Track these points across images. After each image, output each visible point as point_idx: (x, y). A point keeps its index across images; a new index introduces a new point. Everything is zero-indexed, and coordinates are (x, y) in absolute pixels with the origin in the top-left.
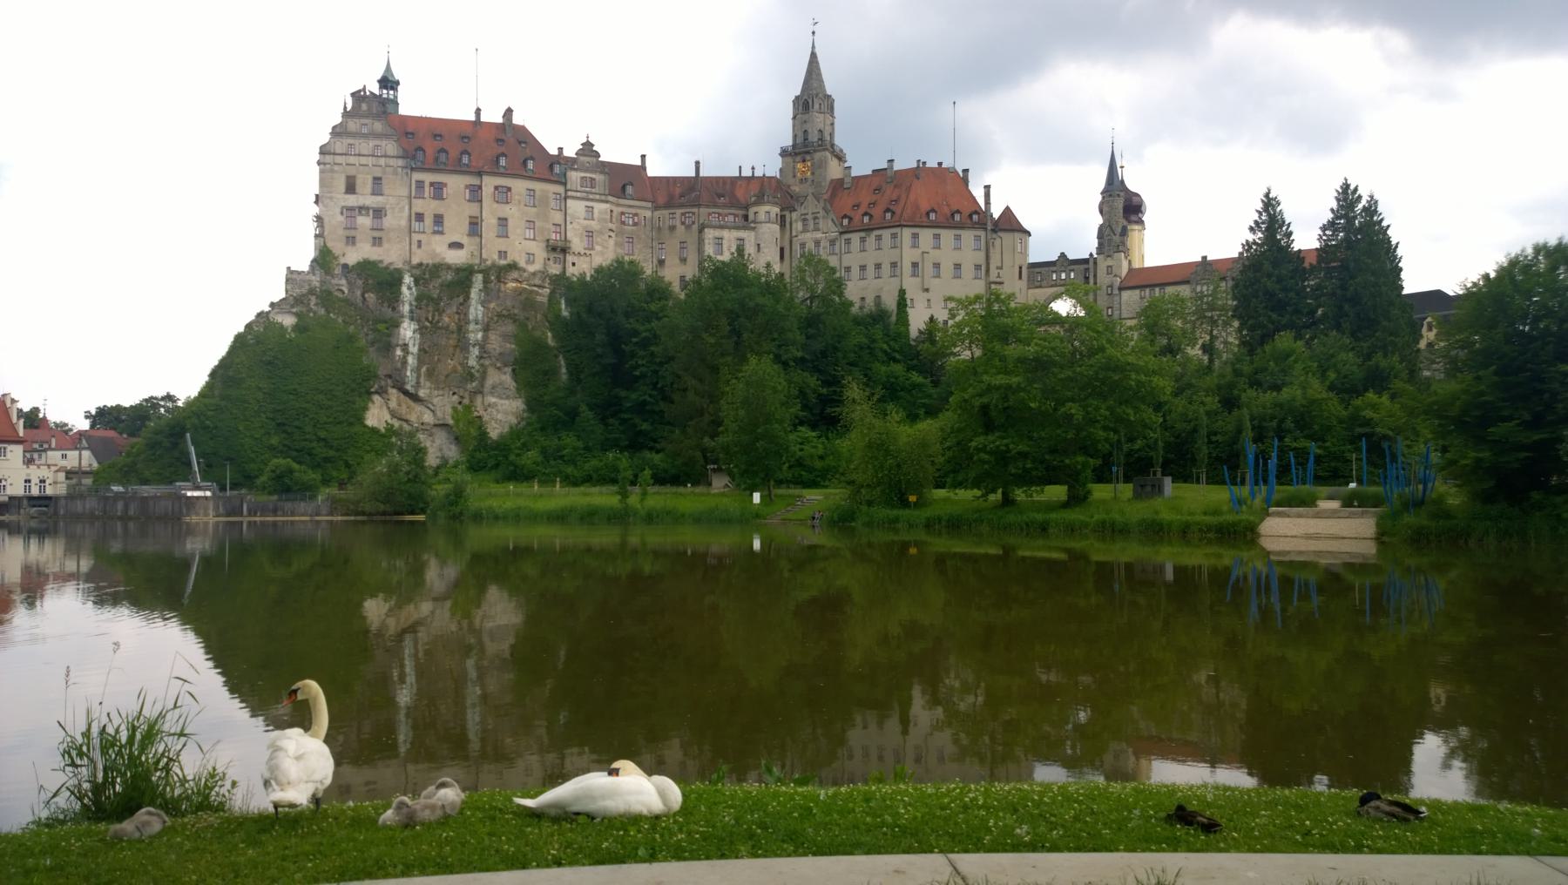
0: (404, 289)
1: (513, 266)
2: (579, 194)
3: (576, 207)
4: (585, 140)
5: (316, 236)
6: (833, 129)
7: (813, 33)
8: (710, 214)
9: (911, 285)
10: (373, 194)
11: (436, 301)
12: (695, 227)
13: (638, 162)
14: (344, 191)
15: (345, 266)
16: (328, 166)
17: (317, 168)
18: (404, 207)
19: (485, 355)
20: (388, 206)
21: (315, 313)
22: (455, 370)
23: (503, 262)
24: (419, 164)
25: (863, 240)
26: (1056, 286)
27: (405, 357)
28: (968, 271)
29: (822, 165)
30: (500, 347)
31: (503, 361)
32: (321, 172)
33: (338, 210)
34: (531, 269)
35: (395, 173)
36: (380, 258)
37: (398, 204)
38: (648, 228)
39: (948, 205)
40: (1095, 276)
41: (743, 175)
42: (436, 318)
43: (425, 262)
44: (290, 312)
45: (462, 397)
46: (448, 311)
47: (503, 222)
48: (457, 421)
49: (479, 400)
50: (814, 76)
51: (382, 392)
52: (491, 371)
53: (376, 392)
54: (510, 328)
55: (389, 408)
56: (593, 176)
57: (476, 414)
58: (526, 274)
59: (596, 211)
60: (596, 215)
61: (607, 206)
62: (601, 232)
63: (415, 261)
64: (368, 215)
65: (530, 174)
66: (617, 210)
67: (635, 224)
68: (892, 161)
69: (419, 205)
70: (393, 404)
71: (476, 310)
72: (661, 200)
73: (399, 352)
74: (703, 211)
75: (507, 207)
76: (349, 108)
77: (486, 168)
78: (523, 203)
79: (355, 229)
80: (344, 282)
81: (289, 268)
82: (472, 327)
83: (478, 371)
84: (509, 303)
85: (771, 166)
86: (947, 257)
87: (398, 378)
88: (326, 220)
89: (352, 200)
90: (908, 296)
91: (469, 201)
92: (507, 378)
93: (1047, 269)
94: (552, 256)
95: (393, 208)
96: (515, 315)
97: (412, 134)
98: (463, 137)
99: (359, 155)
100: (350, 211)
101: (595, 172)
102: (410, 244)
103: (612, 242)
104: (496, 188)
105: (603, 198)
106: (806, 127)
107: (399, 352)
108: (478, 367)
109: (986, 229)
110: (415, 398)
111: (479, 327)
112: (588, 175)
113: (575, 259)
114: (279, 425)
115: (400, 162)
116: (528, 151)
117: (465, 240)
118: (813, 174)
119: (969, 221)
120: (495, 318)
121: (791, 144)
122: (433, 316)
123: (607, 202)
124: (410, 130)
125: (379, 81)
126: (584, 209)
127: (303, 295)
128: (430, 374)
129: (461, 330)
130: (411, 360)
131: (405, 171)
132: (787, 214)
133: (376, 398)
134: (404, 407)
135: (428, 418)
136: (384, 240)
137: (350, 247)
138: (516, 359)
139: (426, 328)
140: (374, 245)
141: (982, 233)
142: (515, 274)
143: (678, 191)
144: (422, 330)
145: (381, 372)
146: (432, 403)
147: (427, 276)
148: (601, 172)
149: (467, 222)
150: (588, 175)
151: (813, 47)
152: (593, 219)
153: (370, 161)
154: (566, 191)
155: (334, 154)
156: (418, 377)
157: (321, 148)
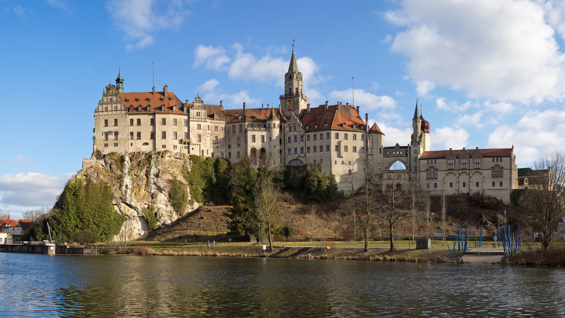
0: (126, 163)
15: (104, 155)
23: (163, 150)
26: (394, 157)
29: (297, 103)
34: (175, 151)
37: (123, 129)
40: (410, 154)
56: (200, 111)
59: (202, 126)
68: (327, 102)
69: (131, 129)
71: (153, 171)
85: (276, 104)
93: (391, 150)
95: (121, 131)
118: (294, 107)
121: (284, 94)
123: (206, 122)
126: (197, 125)
127: (88, 168)
137: (106, 148)
140: (115, 145)
142: (168, 154)
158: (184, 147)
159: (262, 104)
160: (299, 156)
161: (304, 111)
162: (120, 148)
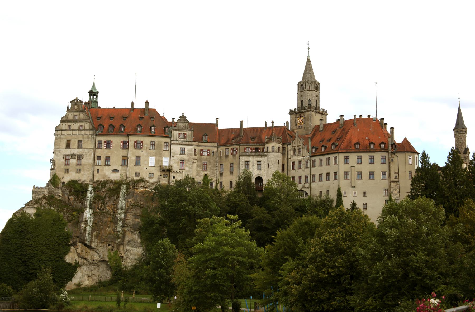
0: (88, 194)
1: (142, 180)
2: (177, 142)
3: (176, 149)
4: (181, 115)
5: (51, 169)
6: (318, 99)
7: (309, 49)
8: (245, 148)
9: (344, 185)
10: (78, 148)
11: (104, 199)
12: (237, 155)
13: (215, 122)
14: (65, 147)
15: (64, 183)
16: (59, 136)
17: (54, 136)
18: (91, 154)
19: (125, 225)
20: (84, 154)
21: (44, 207)
22: (110, 233)
23: (136, 178)
24: (100, 132)
25: (321, 160)
27: (85, 227)
28: (378, 175)
31: (135, 228)
32: (56, 139)
33: (62, 156)
34: (152, 181)
35: (88, 138)
37: (89, 152)
38: (215, 157)
41: (267, 126)
42: (103, 207)
43: (100, 180)
44: (33, 207)
45: (113, 247)
46: (109, 204)
47: (138, 158)
48: (110, 259)
49: (121, 248)
50: (308, 72)
51: (74, 244)
52: (127, 234)
53: (71, 245)
54: (138, 211)
55: (77, 252)
56: (185, 132)
58: (148, 184)
59: (186, 150)
60: (186, 151)
62: (188, 161)
63: (96, 179)
64: (75, 158)
65: (153, 134)
66: (198, 149)
67: (208, 155)
68: (342, 116)
69: (99, 152)
70: (79, 251)
71: (122, 203)
72: (223, 142)
73: (83, 225)
74: (242, 147)
75: (140, 151)
76: (69, 108)
77: (131, 133)
79: (69, 165)
80: (60, 191)
81: (34, 186)
82: (119, 211)
83: (121, 234)
84: (138, 199)
86: (365, 168)
87: (82, 238)
88: (56, 161)
89: (68, 152)
90: (342, 190)
91: (122, 149)
92: (136, 237)
95: (86, 154)
96: (141, 204)
98: (124, 117)
99: (73, 130)
100: (67, 157)
101: (186, 130)
103: (195, 165)
104: (136, 142)
105: (190, 143)
106: (303, 98)
107: (83, 225)
108: (121, 231)
109: (388, 152)
110: (90, 247)
111: (123, 211)
112: (182, 132)
113: (175, 175)
114: (23, 261)
115: (91, 132)
117: (120, 168)
118: (304, 123)
119: (379, 148)
120: (131, 207)
121: (297, 107)
122: (101, 206)
123: (192, 145)
125: (89, 92)
127: (40, 199)
128: (97, 236)
129: (115, 211)
130: (88, 228)
131: (92, 136)
132: (286, 146)
134: (84, 252)
135: (96, 257)
136: (82, 170)
137: (66, 174)
138: (140, 227)
139: (97, 212)
140: (77, 172)
141: (386, 154)
142: (143, 184)
143: (232, 136)
144: (95, 214)
145: (74, 235)
146: (98, 250)
148: (189, 131)
150: (182, 132)
151: (308, 56)
152: (184, 154)
153: (77, 132)
154: (171, 141)
155: (62, 130)
156: (92, 237)
157: (56, 128)
158: (162, 175)
159: (266, 122)
160: (303, 187)
161: (317, 128)
162: (83, 175)
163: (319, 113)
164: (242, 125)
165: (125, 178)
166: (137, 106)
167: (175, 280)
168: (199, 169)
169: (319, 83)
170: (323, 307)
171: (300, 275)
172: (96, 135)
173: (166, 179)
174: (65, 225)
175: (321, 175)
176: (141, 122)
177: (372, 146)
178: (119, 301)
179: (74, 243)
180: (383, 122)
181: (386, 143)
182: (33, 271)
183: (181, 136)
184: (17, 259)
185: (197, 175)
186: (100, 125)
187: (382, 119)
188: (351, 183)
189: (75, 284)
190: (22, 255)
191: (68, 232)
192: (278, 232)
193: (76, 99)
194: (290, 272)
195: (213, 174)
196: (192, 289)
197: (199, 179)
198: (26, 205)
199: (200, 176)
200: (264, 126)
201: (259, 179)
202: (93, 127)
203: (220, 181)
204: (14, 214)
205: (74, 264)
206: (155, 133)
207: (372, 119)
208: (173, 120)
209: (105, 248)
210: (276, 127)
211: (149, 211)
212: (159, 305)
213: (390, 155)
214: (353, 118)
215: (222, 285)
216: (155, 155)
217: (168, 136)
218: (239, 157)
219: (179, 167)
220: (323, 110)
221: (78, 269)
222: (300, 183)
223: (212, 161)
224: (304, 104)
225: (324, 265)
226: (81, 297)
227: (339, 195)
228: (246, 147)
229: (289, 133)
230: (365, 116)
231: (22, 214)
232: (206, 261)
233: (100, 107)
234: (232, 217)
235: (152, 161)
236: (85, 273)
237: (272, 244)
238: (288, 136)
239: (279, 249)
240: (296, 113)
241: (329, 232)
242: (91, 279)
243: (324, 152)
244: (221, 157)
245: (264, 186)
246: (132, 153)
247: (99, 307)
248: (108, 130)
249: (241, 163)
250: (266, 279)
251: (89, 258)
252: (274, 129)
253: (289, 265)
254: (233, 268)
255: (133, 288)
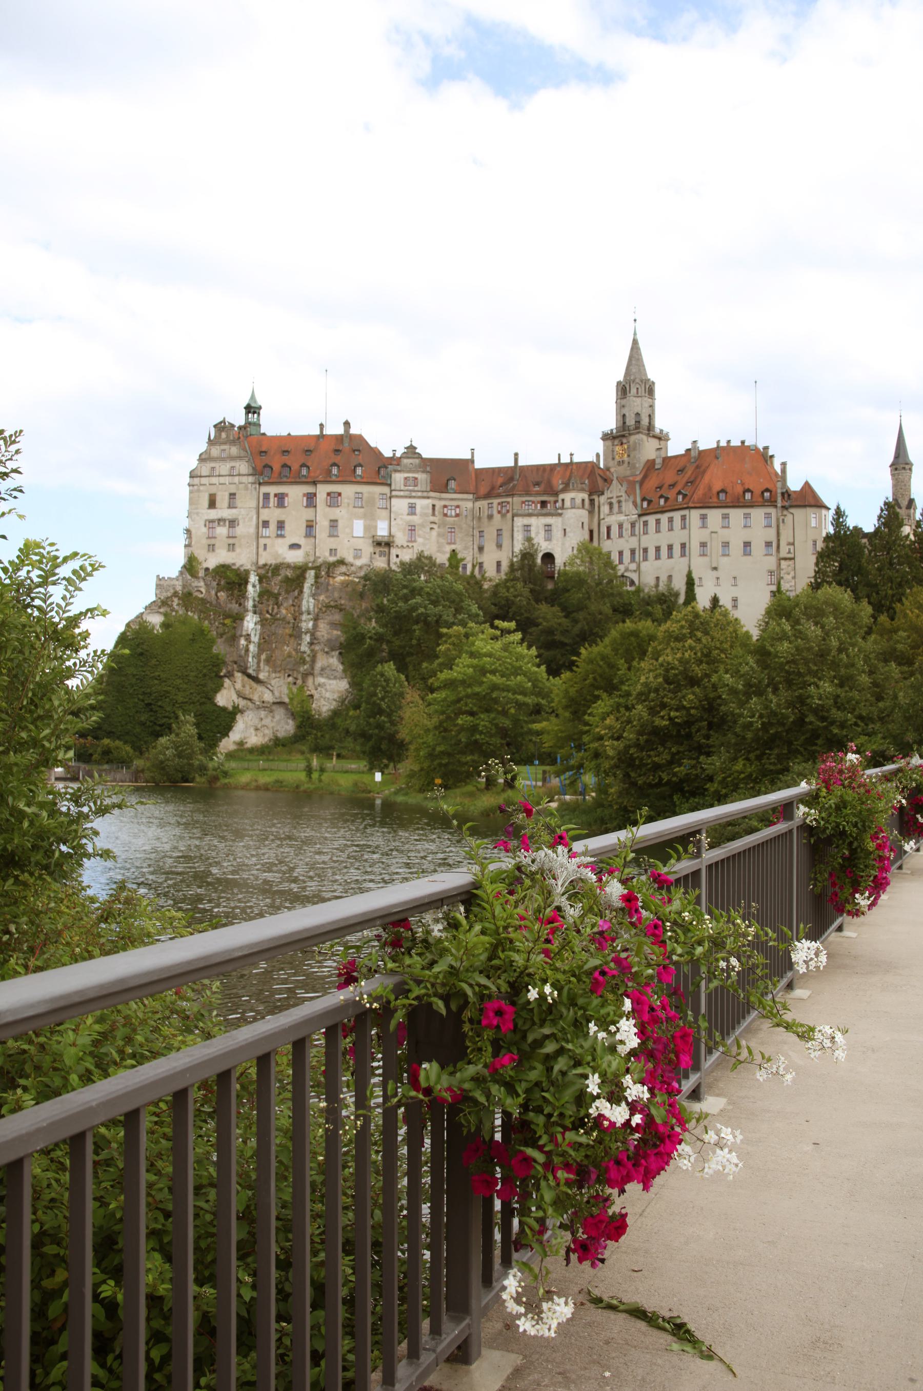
0: (250, 588)
1: (342, 562)
2: (402, 493)
3: (400, 505)
4: (408, 444)
5: (186, 546)
8: (523, 502)
10: (230, 507)
11: (276, 596)
12: (509, 515)
13: (470, 457)
14: (207, 506)
15: (207, 569)
16: (196, 487)
17: (188, 489)
19: (315, 642)
20: (240, 517)
21: (177, 612)
22: (289, 656)
23: (332, 559)
24: (266, 479)
25: (658, 522)
28: (758, 548)
30: (328, 633)
31: (331, 646)
32: (191, 492)
33: (203, 523)
34: (359, 563)
35: (246, 489)
36: (233, 562)
38: (470, 518)
39: (743, 484)
41: (562, 461)
42: (275, 611)
43: (269, 562)
44: (158, 612)
45: (296, 679)
46: (285, 605)
47: (334, 523)
48: (291, 699)
49: (310, 680)
50: (634, 362)
51: (230, 675)
53: (225, 676)
54: (337, 617)
57: (308, 693)
58: (353, 568)
60: (418, 510)
61: (429, 502)
63: (261, 562)
64: (224, 525)
65: (359, 479)
66: (439, 504)
68: (695, 442)
69: (265, 514)
70: (239, 686)
71: (308, 603)
72: (483, 490)
74: (517, 500)
75: (337, 510)
76: (212, 438)
77: (320, 478)
78: (351, 506)
79: (215, 538)
80: (202, 584)
82: (304, 617)
84: (336, 595)
87: (242, 664)
88: (193, 532)
89: (213, 514)
90: (695, 576)
92: (334, 661)
94: (378, 550)
97: (265, 452)
99: (219, 476)
100: (211, 523)
101: (418, 472)
102: (258, 548)
103: (434, 533)
104: (329, 494)
105: (425, 494)
106: (625, 411)
107: (243, 642)
108: (308, 652)
109: (776, 506)
110: (256, 680)
111: (311, 616)
113: (399, 552)
114: (149, 705)
115: (251, 479)
116: (360, 457)
117: (302, 541)
118: (629, 456)
119: (760, 499)
120: (324, 609)
122: (273, 609)
123: (428, 498)
124: (263, 449)
125: (245, 408)
127: (168, 598)
128: (268, 661)
130: (252, 648)
132: (595, 497)
133: (226, 680)
134: (248, 687)
135: (268, 697)
136: (236, 546)
138: (341, 644)
139: (266, 620)
140: (229, 550)
141: (772, 510)
142: (343, 569)
143: (500, 480)
144: (263, 622)
145: (228, 659)
147: (270, 574)
148: (423, 472)
149: (304, 525)
150: (410, 475)
151: (635, 334)
153: (227, 480)
154: (391, 491)
155: (201, 477)
160: (627, 570)
161: (651, 464)
163: (654, 437)
164: (516, 460)
165: (312, 559)
166: (328, 431)
167: (403, 734)
168: (442, 540)
169: (653, 383)
170: (660, 776)
171: (622, 723)
172: (260, 484)
173: (384, 559)
174: (213, 642)
175: (658, 549)
176: (338, 459)
177: (748, 496)
178: (309, 770)
179: (229, 672)
180: (767, 453)
181: (774, 490)
182: (165, 720)
183: (408, 483)
184: (136, 700)
185: (439, 551)
186: (266, 466)
187: (766, 448)
188: (711, 561)
189: (234, 742)
190: (144, 693)
191: (219, 654)
192: (583, 651)
193: (224, 421)
194: (604, 719)
195: (466, 548)
196: (434, 749)
197: (442, 558)
198: (146, 608)
199: (444, 553)
200: (557, 462)
201: (549, 557)
202: (254, 469)
203: (480, 560)
204: (128, 625)
205: (230, 708)
206: (363, 478)
207: (749, 447)
208: (394, 454)
209: (282, 682)
210: (577, 463)
211: (355, 615)
212: (378, 777)
213: (779, 511)
214: (715, 446)
215: (487, 743)
216: (364, 517)
217: (384, 482)
218: (513, 517)
219: (406, 538)
220: (661, 431)
221: (238, 717)
222: (621, 562)
223: (464, 526)
224: (627, 420)
225: (663, 706)
226: (246, 764)
227: (690, 583)
228: (524, 499)
229: (601, 474)
230: (736, 443)
231: (140, 624)
232: (459, 700)
233: (264, 434)
234: (505, 625)
235: (359, 527)
236: (250, 723)
237: (572, 671)
238: (599, 479)
239: (585, 680)
240: (614, 438)
241: (672, 649)
242: (260, 734)
243: (663, 507)
244: (480, 518)
245: (557, 568)
246: (323, 513)
247: (277, 781)
248: (280, 474)
249: (515, 529)
250: (562, 732)
251: (256, 697)
252: (574, 467)
253: (602, 706)
254: (505, 713)
255: (332, 748)
